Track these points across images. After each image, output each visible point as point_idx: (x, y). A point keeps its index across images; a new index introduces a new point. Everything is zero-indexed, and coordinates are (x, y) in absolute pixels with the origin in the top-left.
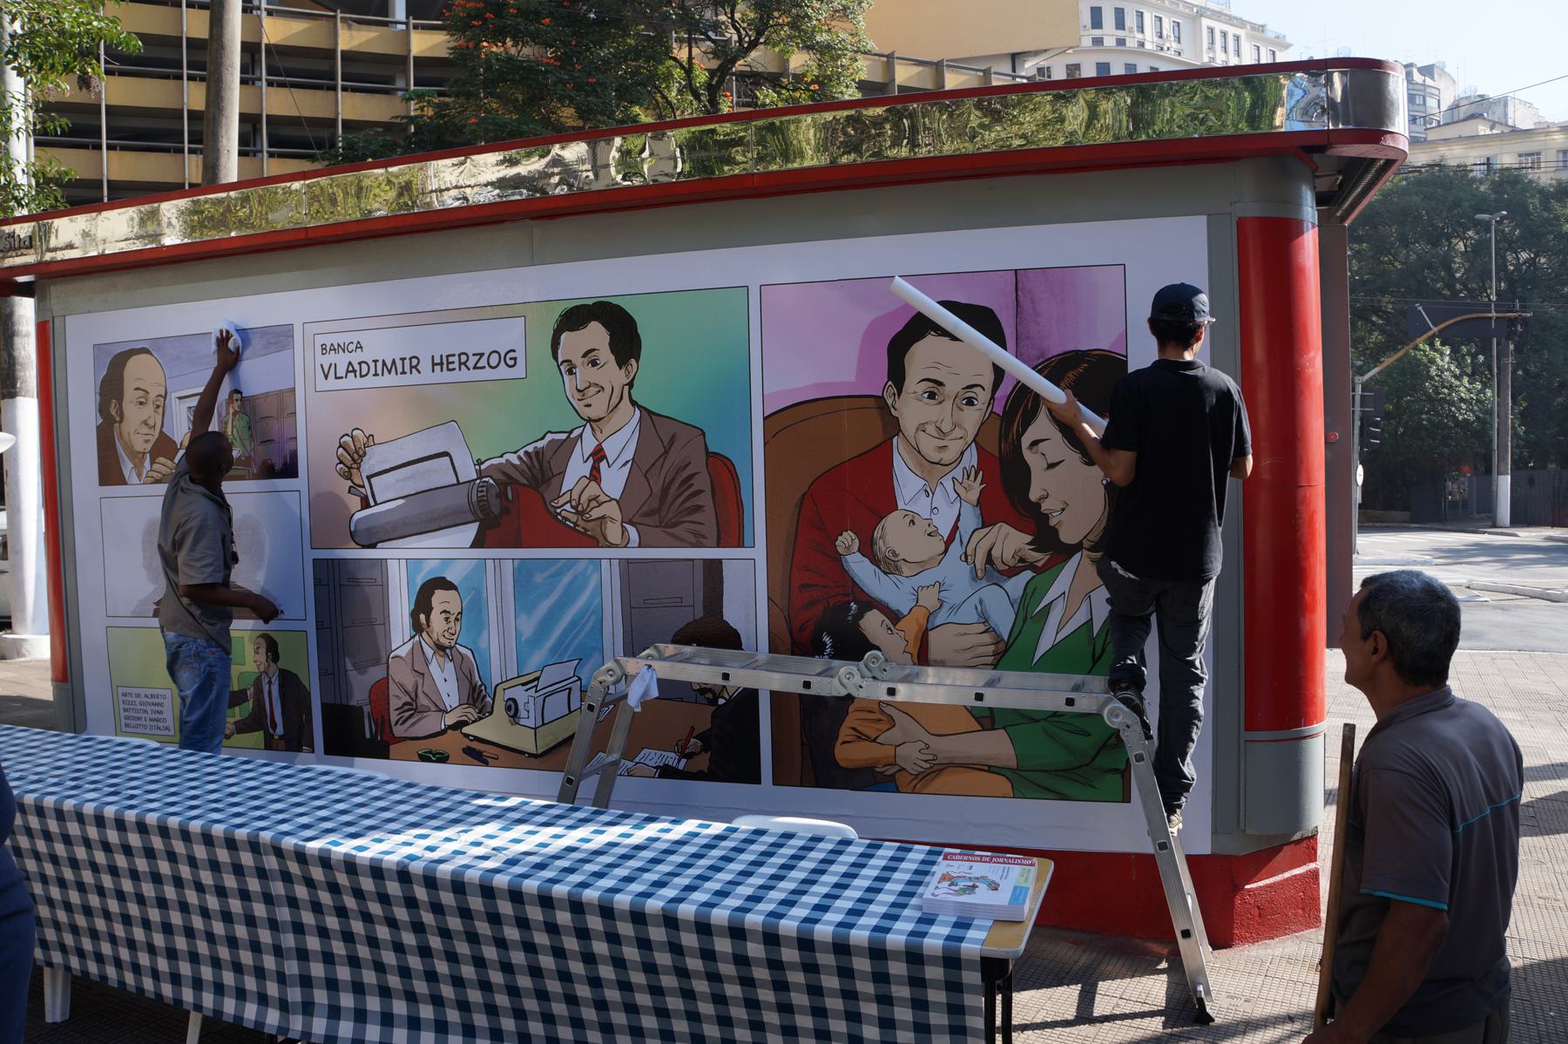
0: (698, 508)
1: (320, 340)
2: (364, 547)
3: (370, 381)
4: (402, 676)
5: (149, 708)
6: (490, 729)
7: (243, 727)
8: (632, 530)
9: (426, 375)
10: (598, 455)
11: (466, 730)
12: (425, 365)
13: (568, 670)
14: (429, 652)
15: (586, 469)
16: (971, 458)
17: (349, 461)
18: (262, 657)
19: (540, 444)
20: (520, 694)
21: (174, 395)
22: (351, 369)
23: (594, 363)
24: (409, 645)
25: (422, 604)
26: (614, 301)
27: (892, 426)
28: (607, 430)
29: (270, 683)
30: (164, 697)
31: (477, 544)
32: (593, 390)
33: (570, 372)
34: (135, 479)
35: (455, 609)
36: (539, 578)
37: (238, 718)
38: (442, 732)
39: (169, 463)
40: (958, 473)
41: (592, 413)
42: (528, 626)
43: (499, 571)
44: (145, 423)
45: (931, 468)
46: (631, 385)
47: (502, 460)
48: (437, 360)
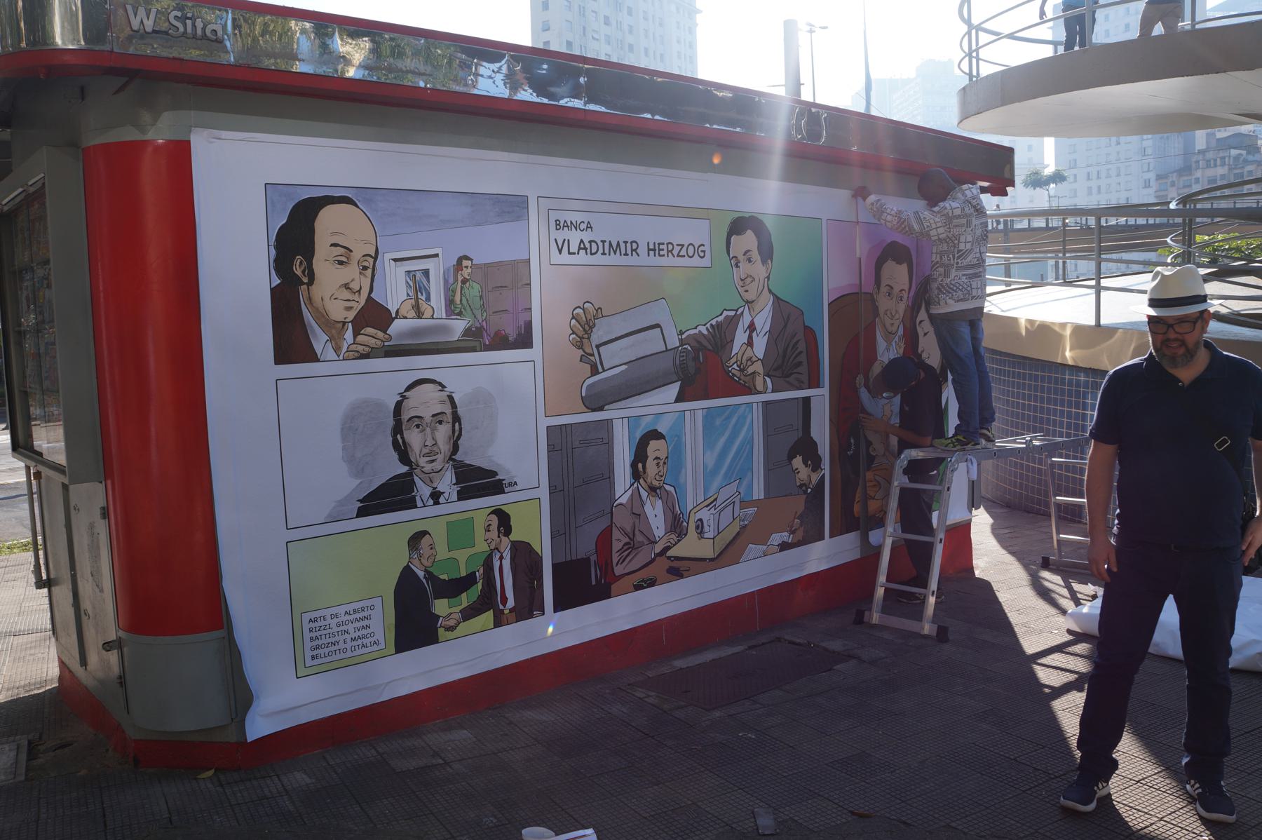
0: (800, 364)
1: (554, 216)
2: (594, 410)
3: (598, 259)
4: (623, 520)
5: (350, 627)
6: (689, 547)
7: (470, 613)
8: (768, 380)
9: (643, 259)
10: (752, 327)
11: (669, 553)
12: (643, 250)
13: (732, 489)
14: (644, 494)
15: (745, 338)
16: (901, 332)
17: (581, 332)
18: (494, 533)
19: (720, 319)
20: (705, 515)
21: (388, 256)
22: (582, 247)
23: (750, 261)
24: (630, 492)
25: (640, 456)
26: (760, 217)
27: (876, 310)
28: (757, 308)
29: (501, 558)
30: (372, 607)
31: (680, 398)
32: (749, 280)
33: (737, 266)
34: (331, 354)
35: (663, 456)
36: (718, 422)
37: (465, 604)
38: (653, 560)
39: (380, 334)
40: (897, 339)
41: (750, 296)
42: (711, 460)
43: (693, 420)
44: (346, 286)
45: (889, 335)
46: (768, 278)
47: (696, 331)
48: (652, 247)
